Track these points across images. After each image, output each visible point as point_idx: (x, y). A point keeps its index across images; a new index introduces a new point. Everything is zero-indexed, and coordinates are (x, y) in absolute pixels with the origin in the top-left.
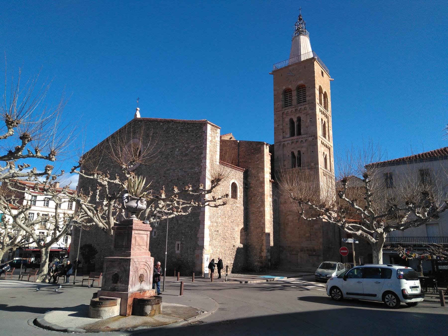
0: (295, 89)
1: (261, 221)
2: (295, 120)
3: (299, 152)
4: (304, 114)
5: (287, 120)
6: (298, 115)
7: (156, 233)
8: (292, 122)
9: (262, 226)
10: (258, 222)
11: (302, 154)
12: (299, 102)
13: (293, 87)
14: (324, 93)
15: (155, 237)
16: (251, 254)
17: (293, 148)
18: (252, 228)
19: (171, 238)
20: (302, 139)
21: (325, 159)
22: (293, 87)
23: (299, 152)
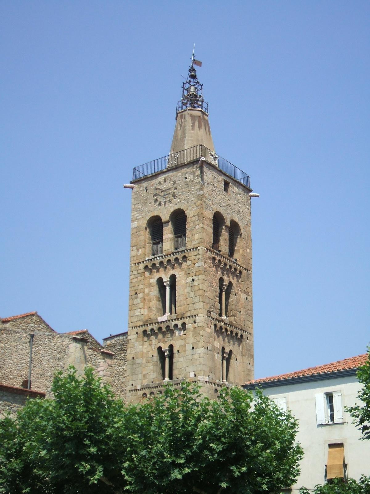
3: (171, 347)
5: (154, 281)
6: (172, 272)
11: (175, 351)
14: (228, 223)
23: (171, 347)
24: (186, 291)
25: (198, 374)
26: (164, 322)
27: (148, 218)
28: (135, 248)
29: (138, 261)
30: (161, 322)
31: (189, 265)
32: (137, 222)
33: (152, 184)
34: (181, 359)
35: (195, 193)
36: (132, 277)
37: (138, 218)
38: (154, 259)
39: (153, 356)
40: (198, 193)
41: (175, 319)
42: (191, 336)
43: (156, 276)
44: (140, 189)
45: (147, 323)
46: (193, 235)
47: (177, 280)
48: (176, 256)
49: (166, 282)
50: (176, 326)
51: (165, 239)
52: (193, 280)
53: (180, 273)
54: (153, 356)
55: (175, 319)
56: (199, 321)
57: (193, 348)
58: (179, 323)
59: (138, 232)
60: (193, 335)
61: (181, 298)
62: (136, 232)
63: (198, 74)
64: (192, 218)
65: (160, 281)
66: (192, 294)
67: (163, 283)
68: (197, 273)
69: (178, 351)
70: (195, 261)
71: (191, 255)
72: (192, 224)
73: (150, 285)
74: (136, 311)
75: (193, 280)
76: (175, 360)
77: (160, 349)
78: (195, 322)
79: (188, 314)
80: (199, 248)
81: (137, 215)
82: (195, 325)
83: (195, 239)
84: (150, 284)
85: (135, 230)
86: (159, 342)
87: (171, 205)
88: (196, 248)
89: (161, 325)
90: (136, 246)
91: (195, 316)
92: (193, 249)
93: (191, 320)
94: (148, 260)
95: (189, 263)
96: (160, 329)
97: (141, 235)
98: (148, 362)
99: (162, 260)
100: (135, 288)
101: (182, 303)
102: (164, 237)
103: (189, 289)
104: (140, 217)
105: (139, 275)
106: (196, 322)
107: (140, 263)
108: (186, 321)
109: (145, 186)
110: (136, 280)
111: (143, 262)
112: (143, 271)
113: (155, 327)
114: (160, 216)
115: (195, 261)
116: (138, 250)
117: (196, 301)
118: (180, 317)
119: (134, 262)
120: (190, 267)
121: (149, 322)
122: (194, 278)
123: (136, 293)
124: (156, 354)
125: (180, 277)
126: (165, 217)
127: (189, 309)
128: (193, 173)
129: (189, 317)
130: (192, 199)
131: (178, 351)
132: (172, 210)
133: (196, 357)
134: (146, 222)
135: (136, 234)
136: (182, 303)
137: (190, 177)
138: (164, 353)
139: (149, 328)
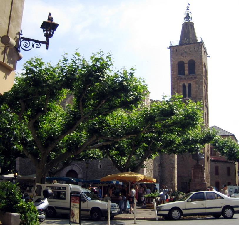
0: (187, 62)
1: (171, 160)
2: (187, 85)
4: (194, 82)
5: (181, 84)
6: (189, 82)
7: (101, 166)
8: (184, 86)
9: (173, 163)
10: (170, 160)
12: (190, 73)
13: (186, 60)
15: (100, 169)
16: (164, 182)
18: (165, 164)
19: (116, 170)
21: (206, 114)
22: (186, 60)
46: (199, 70)
47: (192, 85)
52: (199, 86)
53: (193, 83)
65: (184, 86)
73: (180, 86)
75: (199, 86)
95: (197, 80)
103: (197, 89)
112: (176, 80)
122: (199, 85)
123: (174, 88)
132: (189, 60)
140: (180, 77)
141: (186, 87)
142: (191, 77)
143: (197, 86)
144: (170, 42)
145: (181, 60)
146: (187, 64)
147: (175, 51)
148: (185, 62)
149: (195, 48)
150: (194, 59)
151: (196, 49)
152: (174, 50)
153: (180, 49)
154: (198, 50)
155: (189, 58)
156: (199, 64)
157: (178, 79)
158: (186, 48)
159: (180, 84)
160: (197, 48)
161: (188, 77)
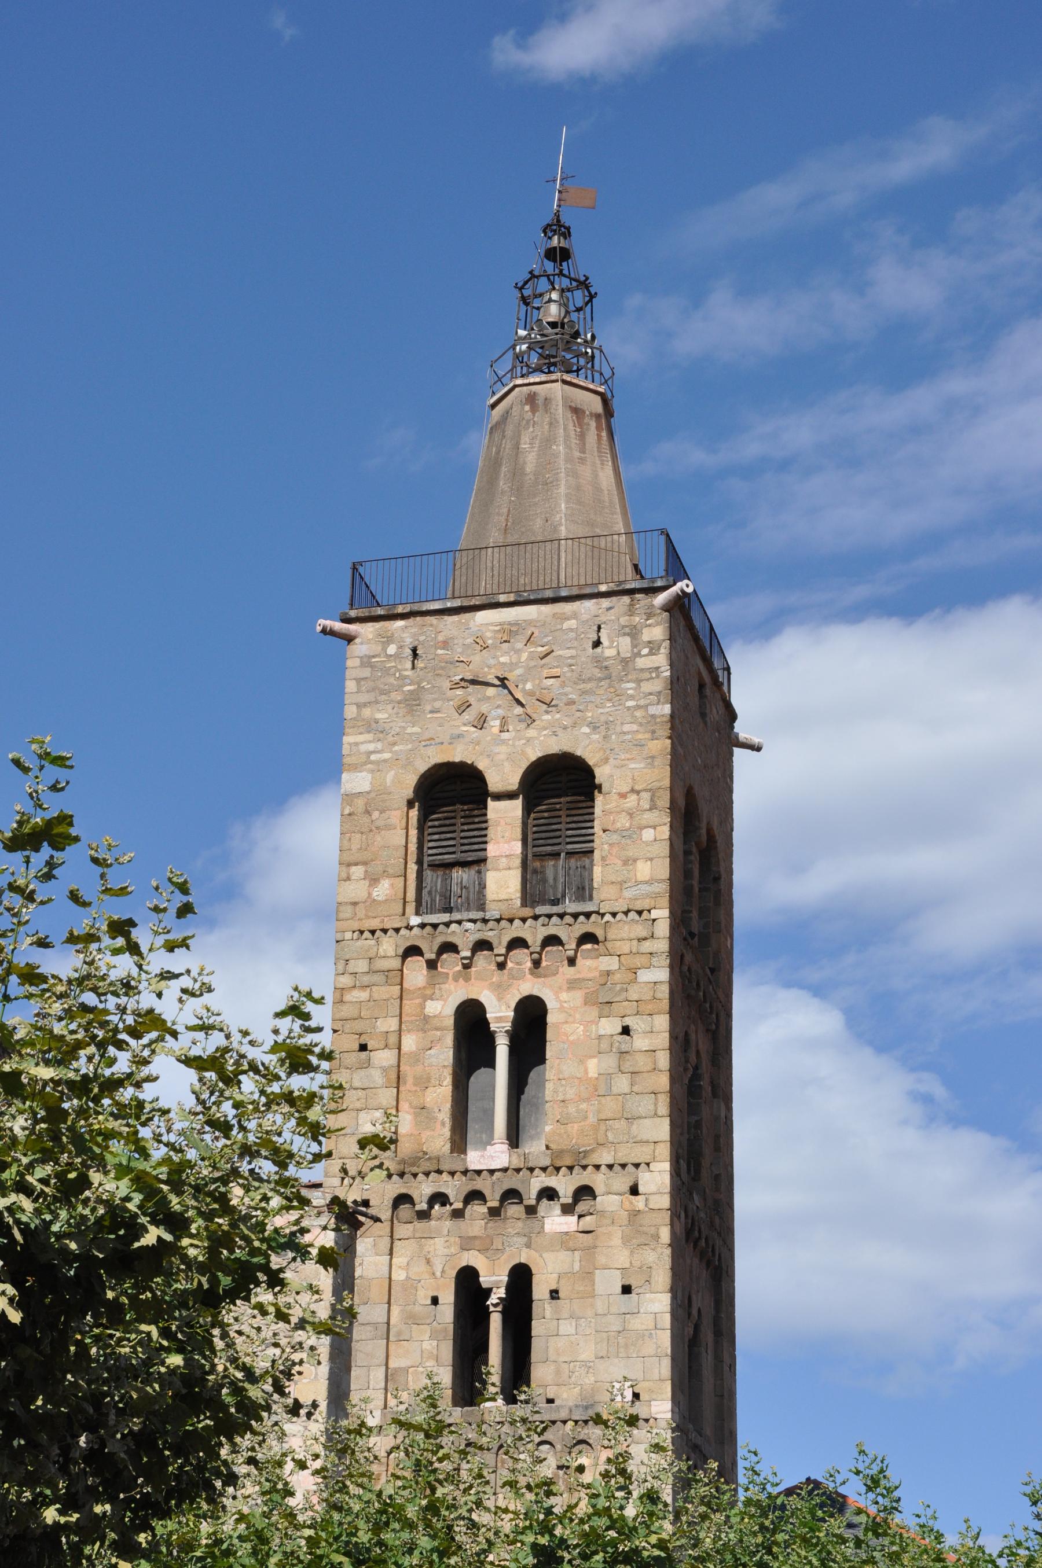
2: (500, 1015)
3: (521, 1278)
4: (573, 985)
5: (443, 1008)
6: (528, 986)
11: (540, 1291)
17: (467, 1243)
20: (552, 1182)
23: (521, 1278)
24: (593, 1067)
25: (651, 1391)
26: (492, 1172)
27: (423, 767)
28: (358, 871)
29: (375, 924)
30: (479, 1172)
31: (608, 973)
32: (372, 771)
33: (440, 638)
34: (567, 1327)
35: (638, 707)
36: (346, 981)
37: (373, 757)
38: (447, 925)
39: (435, 1301)
40: (653, 710)
41: (544, 1169)
42: (617, 1240)
43: (456, 994)
44: (384, 650)
45: (415, 1170)
46: (629, 862)
47: (550, 1019)
48: (552, 930)
49: (499, 1019)
50: (549, 1194)
51: (497, 858)
52: (626, 1031)
53: (564, 996)
54: (435, 1301)
55: (544, 1169)
56: (653, 1188)
57: (627, 1290)
58: (565, 1185)
59: (376, 814)
60: (626, 1240)
61: (571, 1093)
62: (368, 812)
63: (576, 244)
64: (623, 796)
66: (622, 1084)
67: (486, 1023)
68: (650, 1007)
69: (554, 1294)
70: (638, 961)
71: (622, 934)
72: (623, 822)
73: (425, 1022)
74: (362, 1115)
75: (626, 1031)
76: (538, 1327)
77: (467, 1278)
78: (634, 1191)
79: (605, 1157)
80: (655, 914)
81: (371, 747)
82: (639, 1202)
83: (640, 878)
84: (426, 1019)
85: (360, 803)
86: (464, 1249)
87: (531, 733)
88: (640, 913)
89: (479, 1184)
90: (365, 863)
91: (637, 1166)
92: (626, 913)
93: (621, 1181)
94: (423, 926)
95: (610, 963)
96: (475, 1196)
97: (389, 827)
98: (412, 1319)
99: (489, 935)
100: (358, 1026)
101: (572, 1109)
102: (492, 850)
103: (610, 1062)
104: (387, 756)
105: (379, 978)
106: (641, 1189)
107: (385, 931)
108: (598, 1181)
109: (409, 641)
110: (364, 995)
111: (397, 930)
112: (396, 963)
113: (454, 1188)
114: (481, 766)
115: (638, 961)
116: (374, 881)
117: (641, 1111)
118: (569, 1163)
119: (356, 926)
120: (617, 977)
121: (426, 1166)
122: (628, 1021)
123: (363, 1048)
124: (448, 1298)
125: (562, 1009)
126: (503, 772)
127: (611, 1139)
128: (633, 633)
129: (610, 1167)
130: (626, 728)
131: (554, 1294)
132: (534, 754)
133: (637, 1323)
134: (410, 782)
135: (366, 819)
136: (572, 1109)
137: (616, 646)
138: (488, 1292)
139: (422, 1190)
140: (435, 926)
141: (489, 1040)
142: (543, 932)
143: (610, 1026)
144: (354, 569)
145: (458, 755)
146: (510, 796)
147: (397, 656)
148: (495, 782)
149: (597, 644)
150: (584, 745)
151: (608, 651)
152: (392, 649)
153: (445, 645)
154: (625, 662)
155: (541, 742)
156: (632, 800)
157: (413, 951)
158: (508, 634)
159: (433, 1007)
160: (626, 642)
161: (517, 930)
